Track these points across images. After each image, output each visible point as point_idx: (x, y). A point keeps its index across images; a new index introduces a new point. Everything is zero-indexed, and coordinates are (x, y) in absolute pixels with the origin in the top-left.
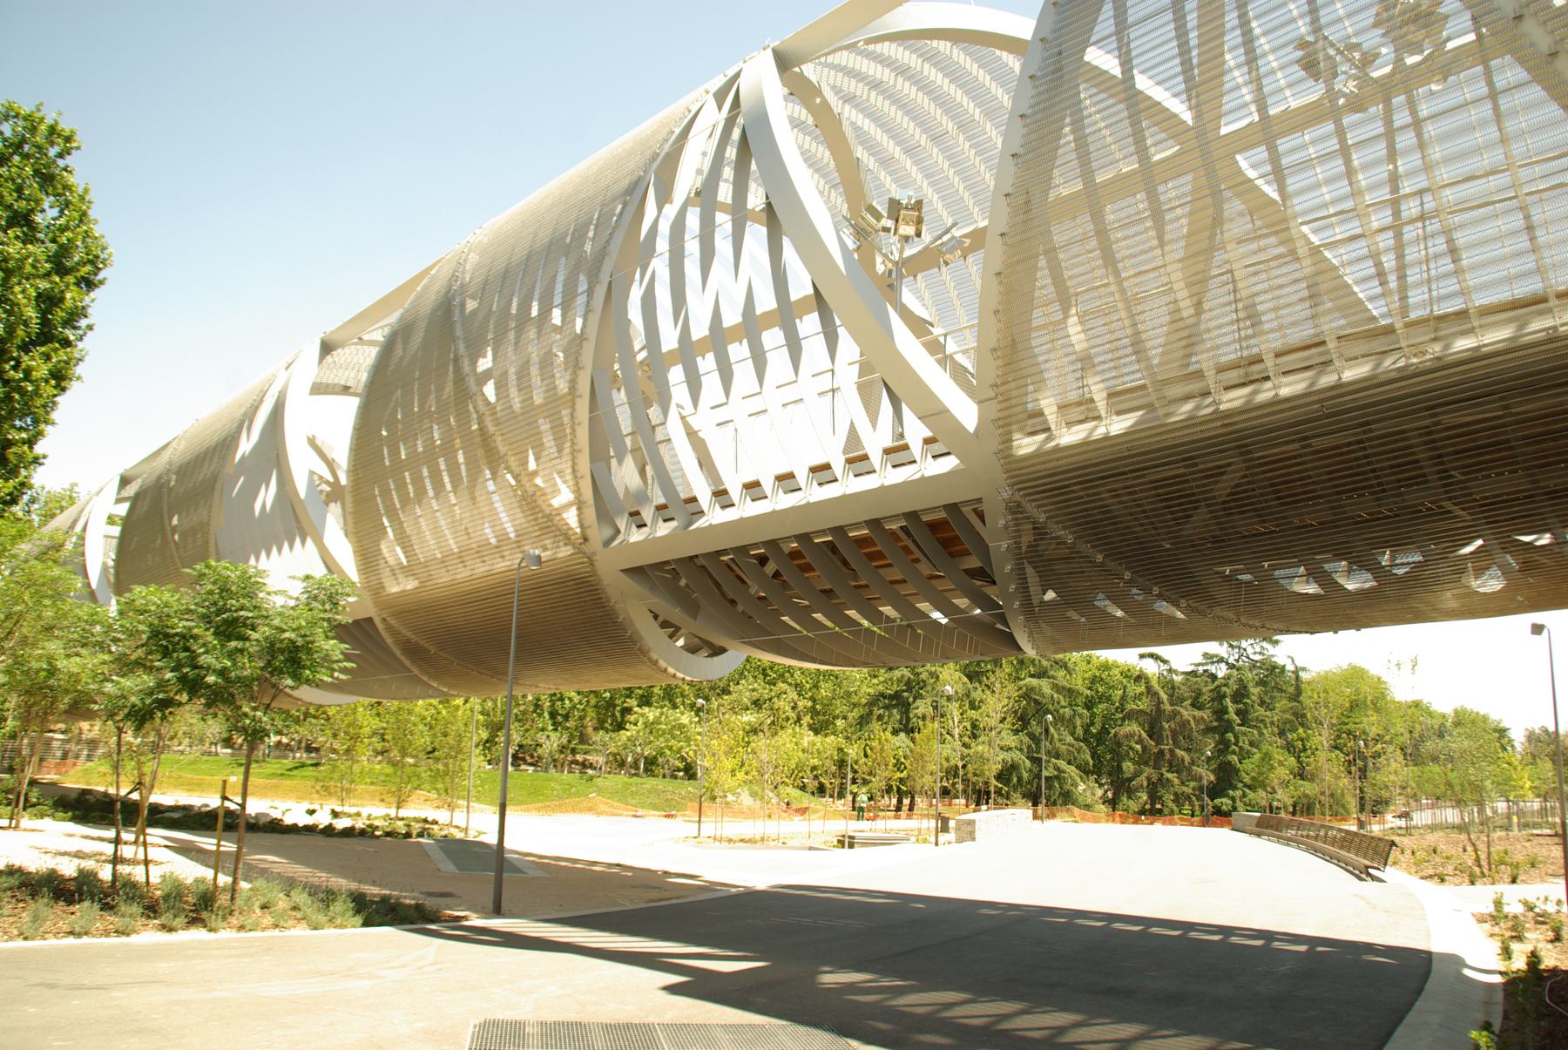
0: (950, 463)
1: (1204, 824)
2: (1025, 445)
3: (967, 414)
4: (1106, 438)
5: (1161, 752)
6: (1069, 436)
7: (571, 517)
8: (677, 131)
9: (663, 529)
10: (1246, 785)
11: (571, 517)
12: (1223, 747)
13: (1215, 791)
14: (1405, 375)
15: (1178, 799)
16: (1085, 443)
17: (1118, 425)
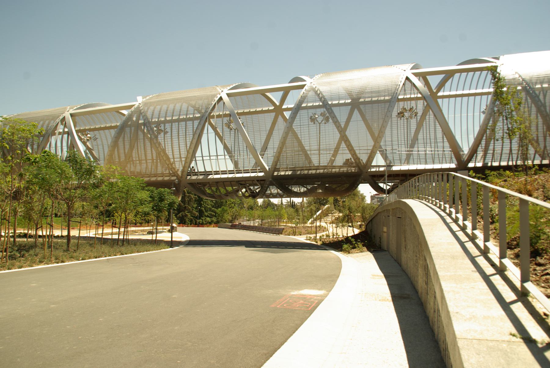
0: (261, 174)
1: (198, 226)
2: (276, 174)
3: (267, 168)
4: (288, 175)
5: (185, 207)
6: (283, 173)
7: (180, 173)
8: (211, 108)
9: (201, 177)
10: (205, 216)
11: (180, 173)
12: (200, 205)
13: (200, 217)
14: (327, 173)
15: (191, 221)
16: (285, 175)
17: (290, 173)
